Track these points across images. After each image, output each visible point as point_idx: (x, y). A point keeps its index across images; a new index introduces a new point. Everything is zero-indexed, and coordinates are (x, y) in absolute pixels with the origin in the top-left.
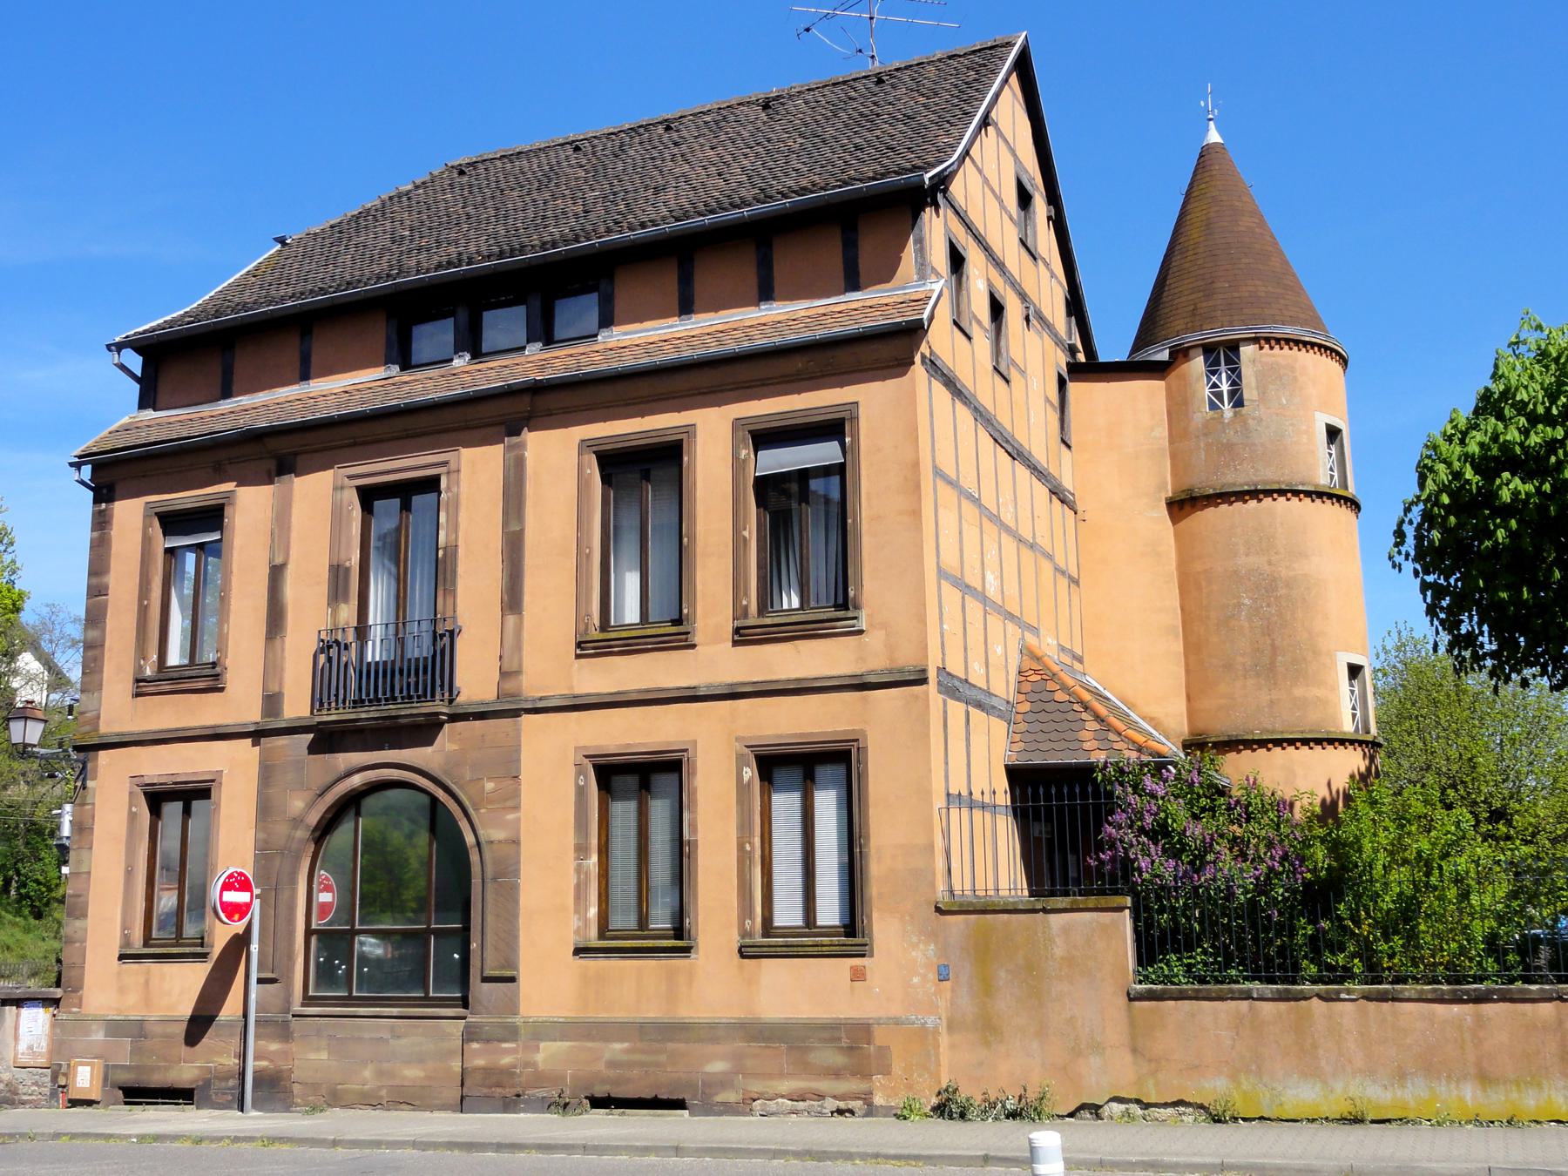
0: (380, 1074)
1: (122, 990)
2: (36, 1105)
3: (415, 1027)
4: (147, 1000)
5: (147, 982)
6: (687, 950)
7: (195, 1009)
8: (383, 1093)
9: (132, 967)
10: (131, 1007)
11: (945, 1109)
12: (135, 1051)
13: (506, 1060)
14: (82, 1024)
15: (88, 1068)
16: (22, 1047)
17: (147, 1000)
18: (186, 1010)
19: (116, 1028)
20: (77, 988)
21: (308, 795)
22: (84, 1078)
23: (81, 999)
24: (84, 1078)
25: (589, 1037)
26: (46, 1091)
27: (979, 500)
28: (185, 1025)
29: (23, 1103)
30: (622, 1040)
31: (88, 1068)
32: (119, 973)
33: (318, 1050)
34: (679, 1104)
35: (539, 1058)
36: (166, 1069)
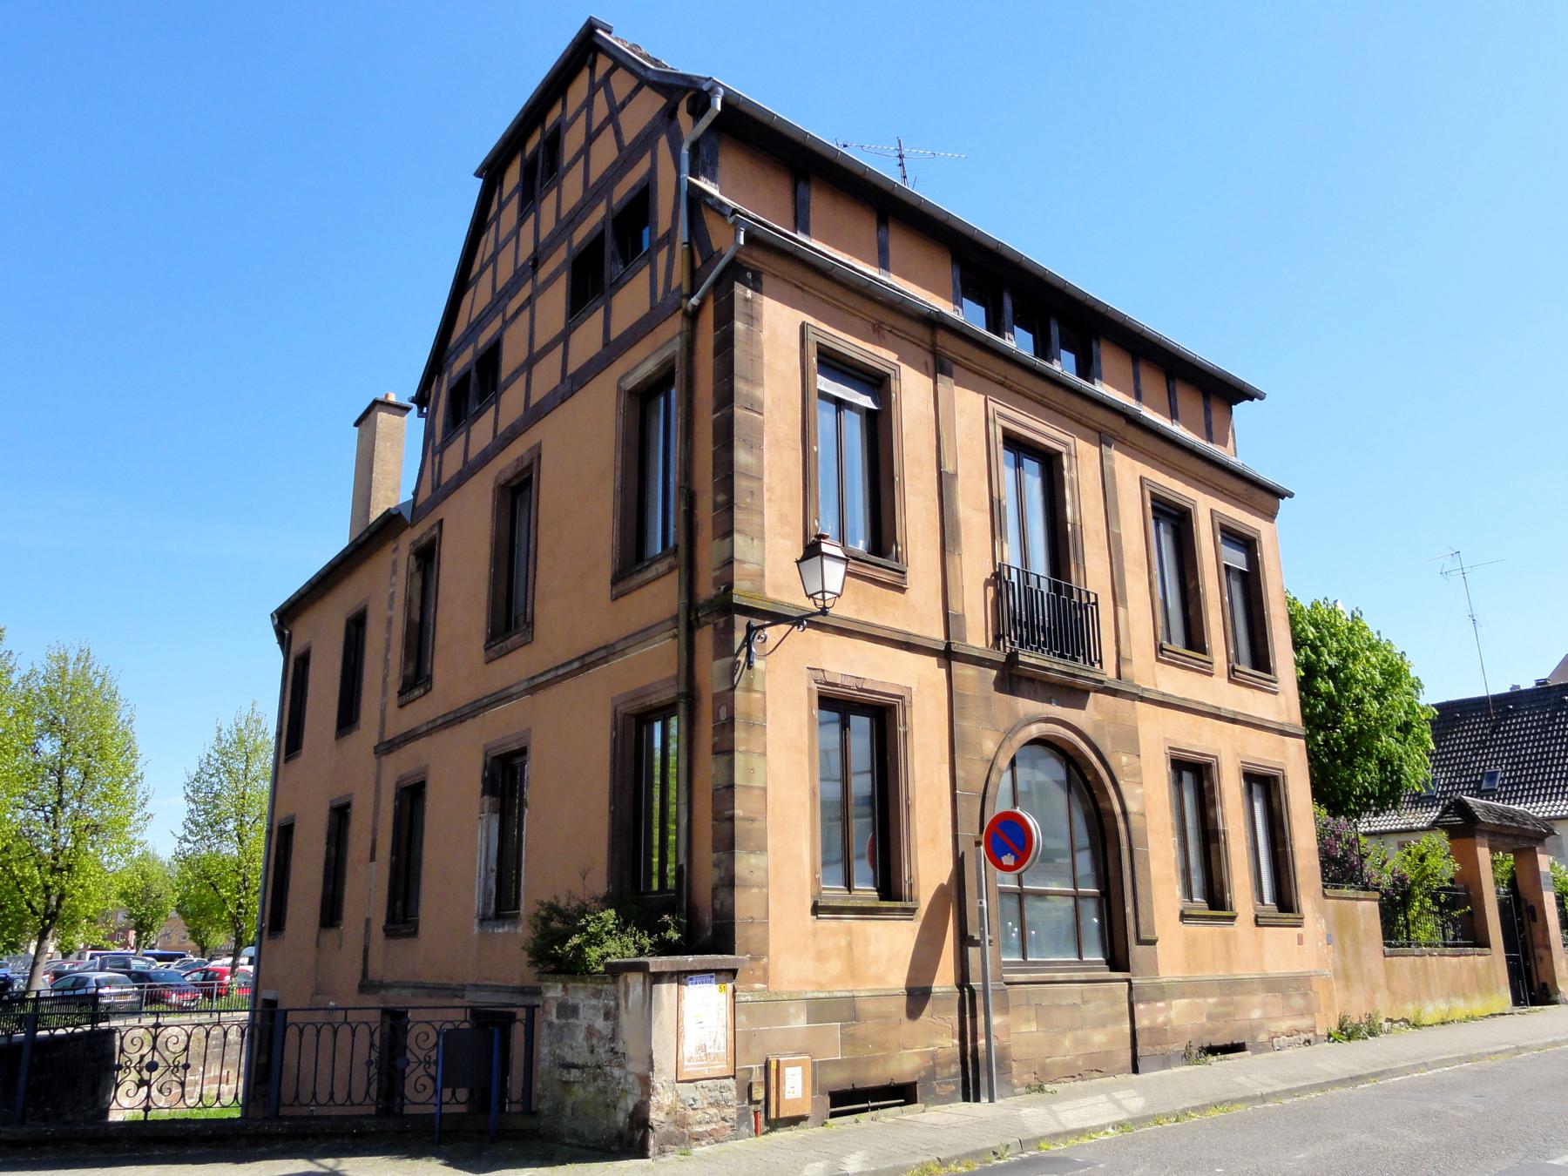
0: (1077, 1043)
1: (821, 957)
2: (714, 1137)
3: (1097, 990)
4: (853, 971)
5: (850, 946)
6: (1233, 918)
7: (909, 979)
8: (1080, 1062)
9: (828, 924)
10: (830, 979)
11: (1347, 1032)
12: (848, 1040)
13: (1161, 1019)
14: (775, 1004)
15: (798, 1070)
16: (689, 1049)
17: (853, 971)
18: (898, 980)
19: (821, 1009)
20: (759, 954)
21: (999, 737)
22: (795, 1087)
23: (766, 970)
24: (795, 1087)
25: (1197, 995)
26: (731, 1112)
27: (882, 221)
28: (904, 1000)
29: (698, 1138)
30: (1212, 996)
31: (798, 1070)
32: (815, 934)
33: (1028, 1021)
34: (1237, 1048)
35: (1173, 1014)
36: (886, 1059)
